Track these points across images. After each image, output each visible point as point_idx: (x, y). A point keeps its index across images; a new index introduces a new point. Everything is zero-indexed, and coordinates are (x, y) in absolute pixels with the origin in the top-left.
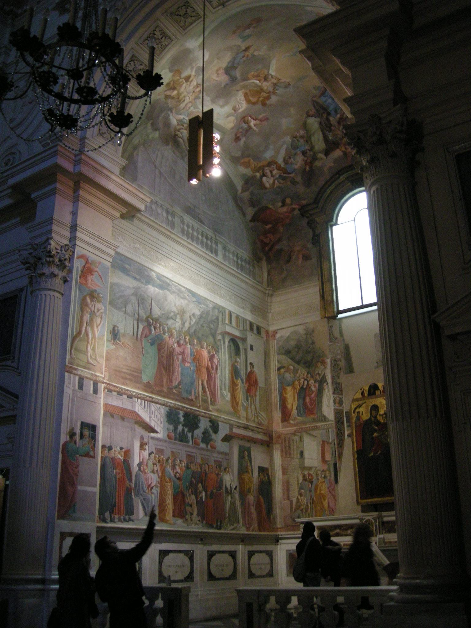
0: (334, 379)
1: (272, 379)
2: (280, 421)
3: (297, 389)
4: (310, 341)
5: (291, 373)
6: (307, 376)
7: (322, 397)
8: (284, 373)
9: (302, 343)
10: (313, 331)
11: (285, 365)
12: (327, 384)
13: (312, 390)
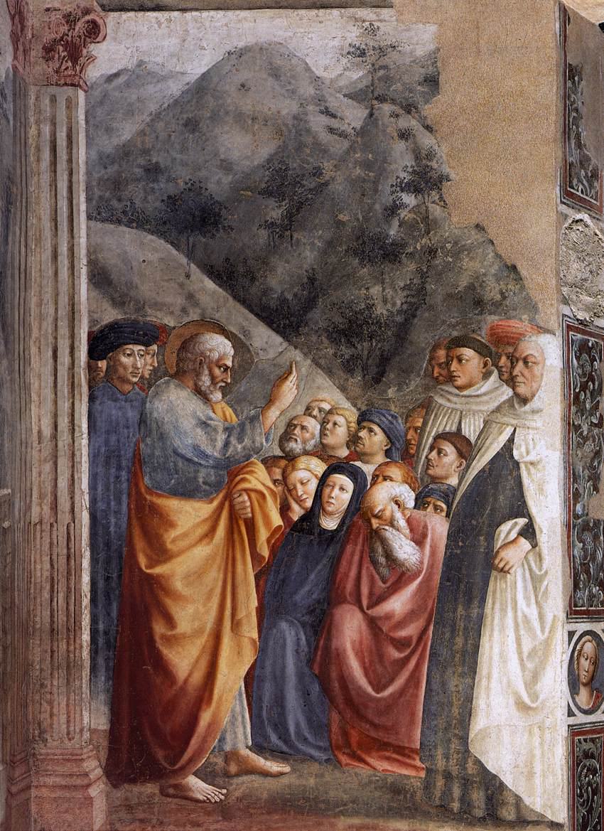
0: (577, 496)
1: (39, 418)
2: (93, 767)
3: (263, 535)
4: (401, 162)
5: (217, 396)
6: (353, 440)
7: (475, 630)
8: (149, 384)
9: (327, 165)
10: (432, 82)
11: (155, 317)
12: (529, 532)
13: (389, 555)
